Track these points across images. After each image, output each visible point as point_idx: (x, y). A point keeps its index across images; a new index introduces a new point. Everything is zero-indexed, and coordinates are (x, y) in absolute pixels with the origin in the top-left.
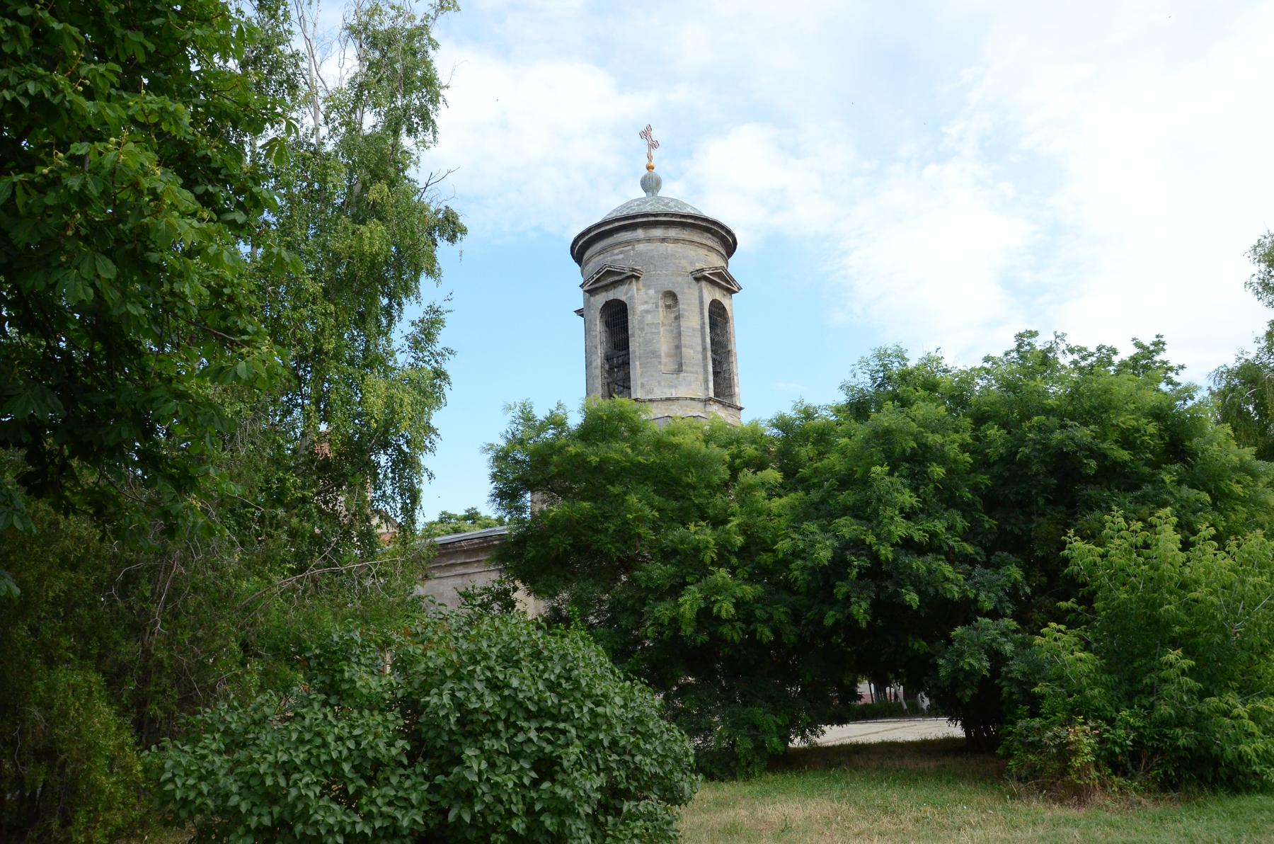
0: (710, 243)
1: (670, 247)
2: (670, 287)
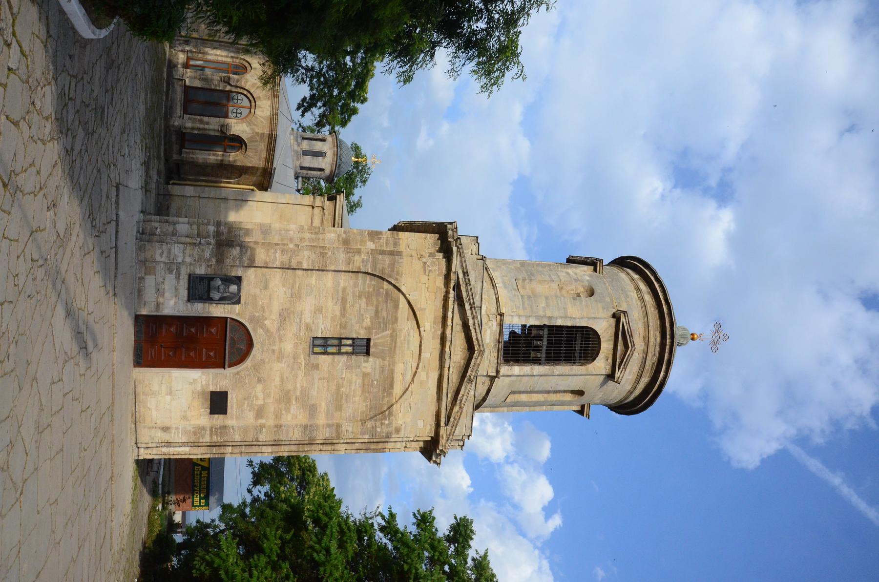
0: (652, 340)
1: (634, 294)
2: (597, 291)
